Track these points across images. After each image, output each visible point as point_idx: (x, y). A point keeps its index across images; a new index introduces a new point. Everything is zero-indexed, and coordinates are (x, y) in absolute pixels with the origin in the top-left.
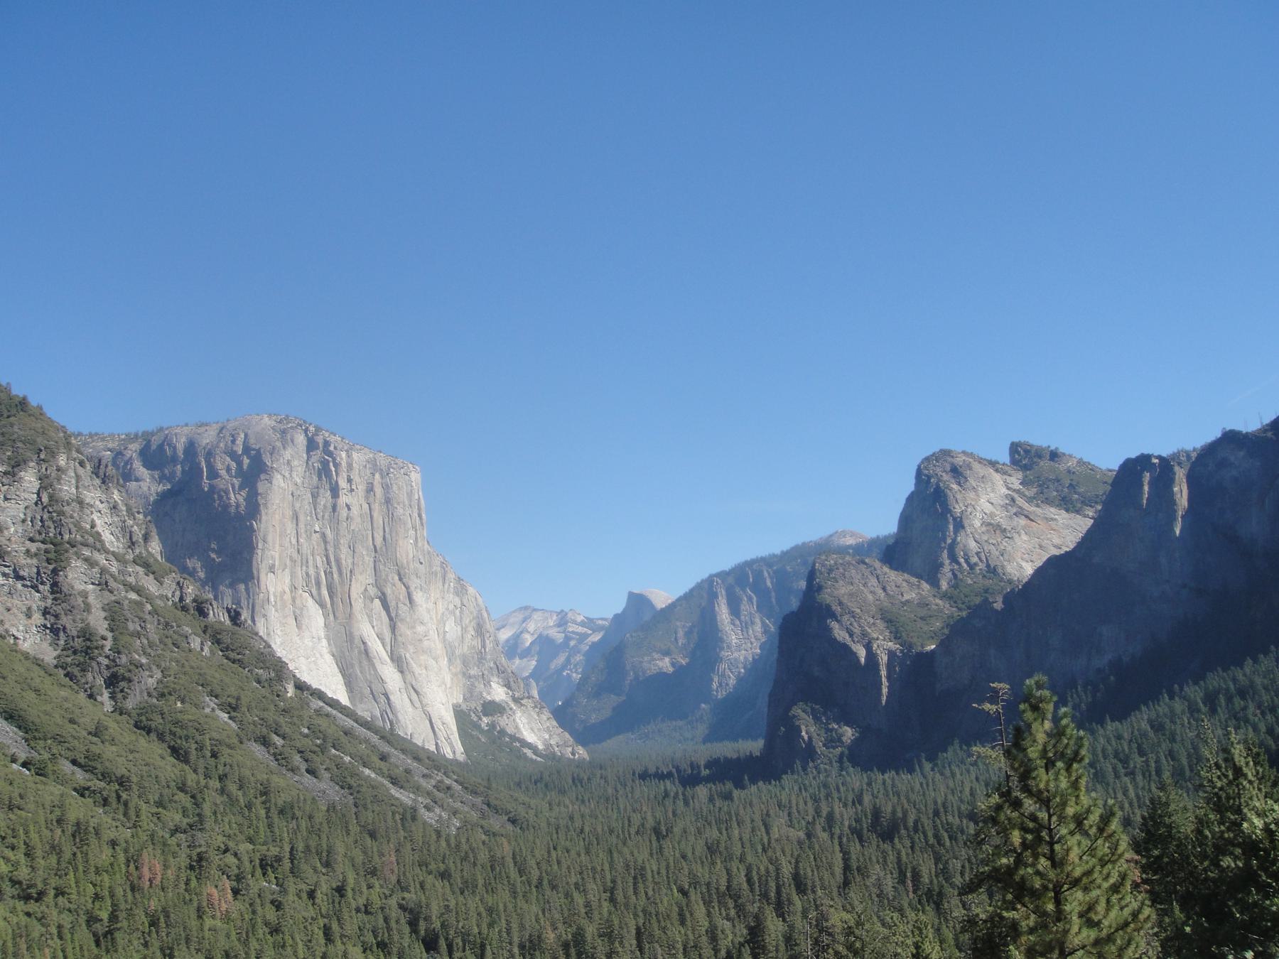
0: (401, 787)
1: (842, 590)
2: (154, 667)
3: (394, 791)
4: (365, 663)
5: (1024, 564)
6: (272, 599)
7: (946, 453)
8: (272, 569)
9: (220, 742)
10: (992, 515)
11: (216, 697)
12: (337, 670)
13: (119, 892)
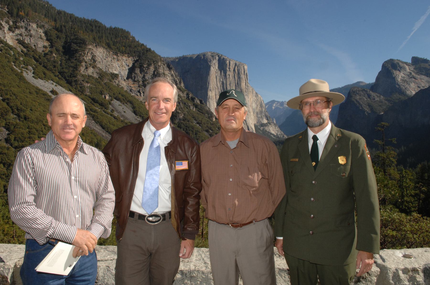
1: (358, 97)
2: (182, 113)
5: (412, 91)
6: (211, 97)
9: (197, 131)
10: (404, 77)
11: (196, 120)
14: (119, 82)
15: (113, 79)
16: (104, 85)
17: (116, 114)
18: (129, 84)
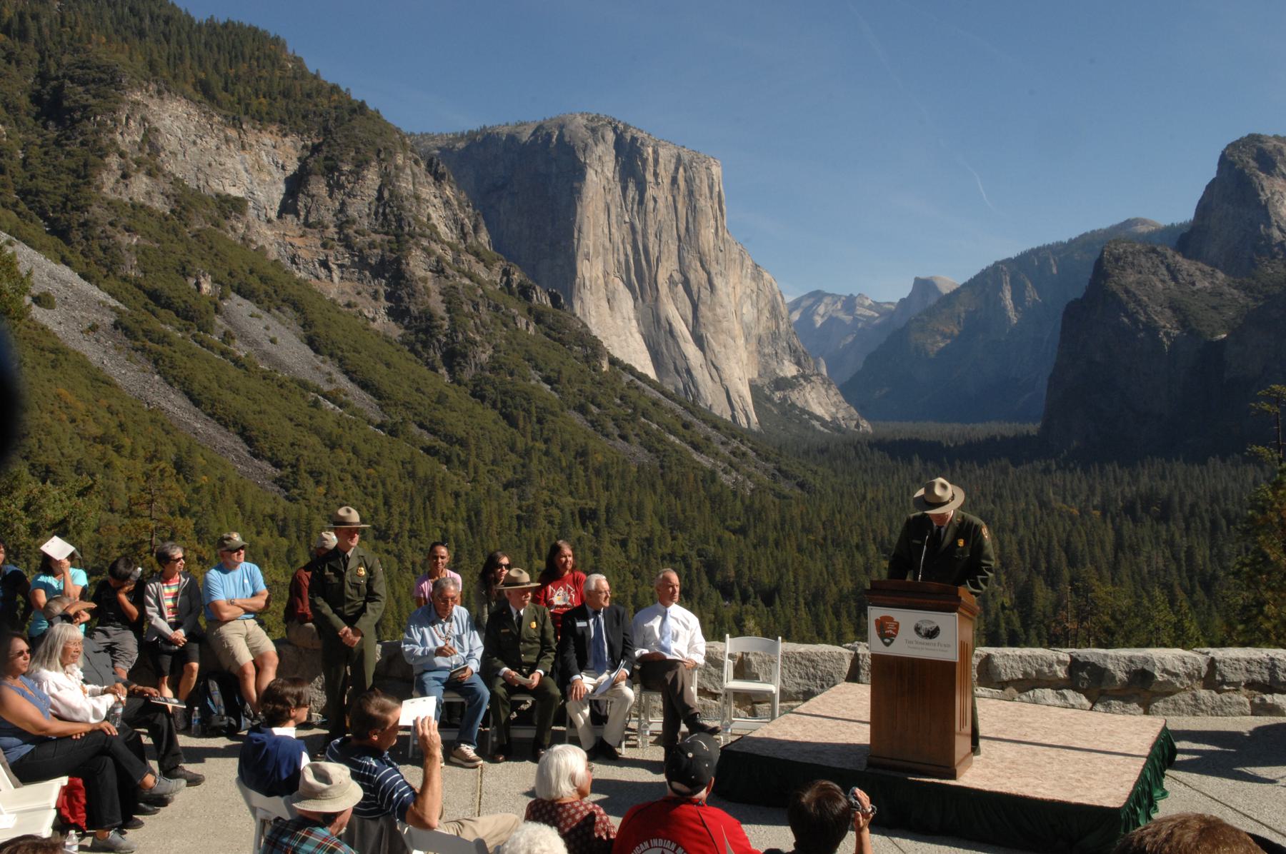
0: (702, 452)
1: (1131, 278)
2: (486, 344)
3: (696, 456)
4: (670, 341)
6: (587, 283)
7: (1254, 139)
8: (587, 257)
9: (545, 409)
11: (541, 370)
12: (645, 347)
13: (462, 537)
14: (248, 227)
15: (227, 218)
16: (194, 240)
17: (240, 349)
18: (285, 234)
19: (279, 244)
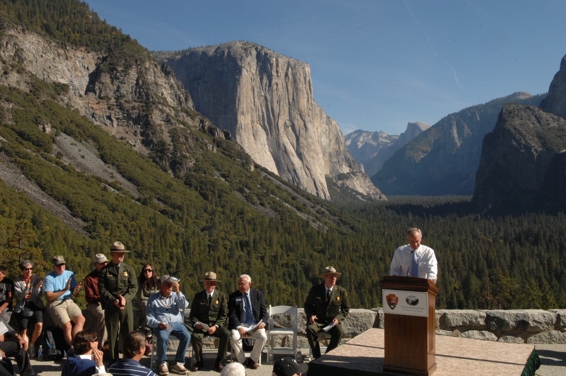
1: (517, 122)
2: (192, 158)
3: (298, 213)
4: (285, 156)
6: (243, 127)
8: (243, 113)
9: (222, 190)
11: (220, 171)
12: (272, 159)
13: (180, 256)
14: (70, 99)
15: (59, 94)
16: (42, 106)
17: (66, 161)
18: (88, 103)
19: (86, 108)
